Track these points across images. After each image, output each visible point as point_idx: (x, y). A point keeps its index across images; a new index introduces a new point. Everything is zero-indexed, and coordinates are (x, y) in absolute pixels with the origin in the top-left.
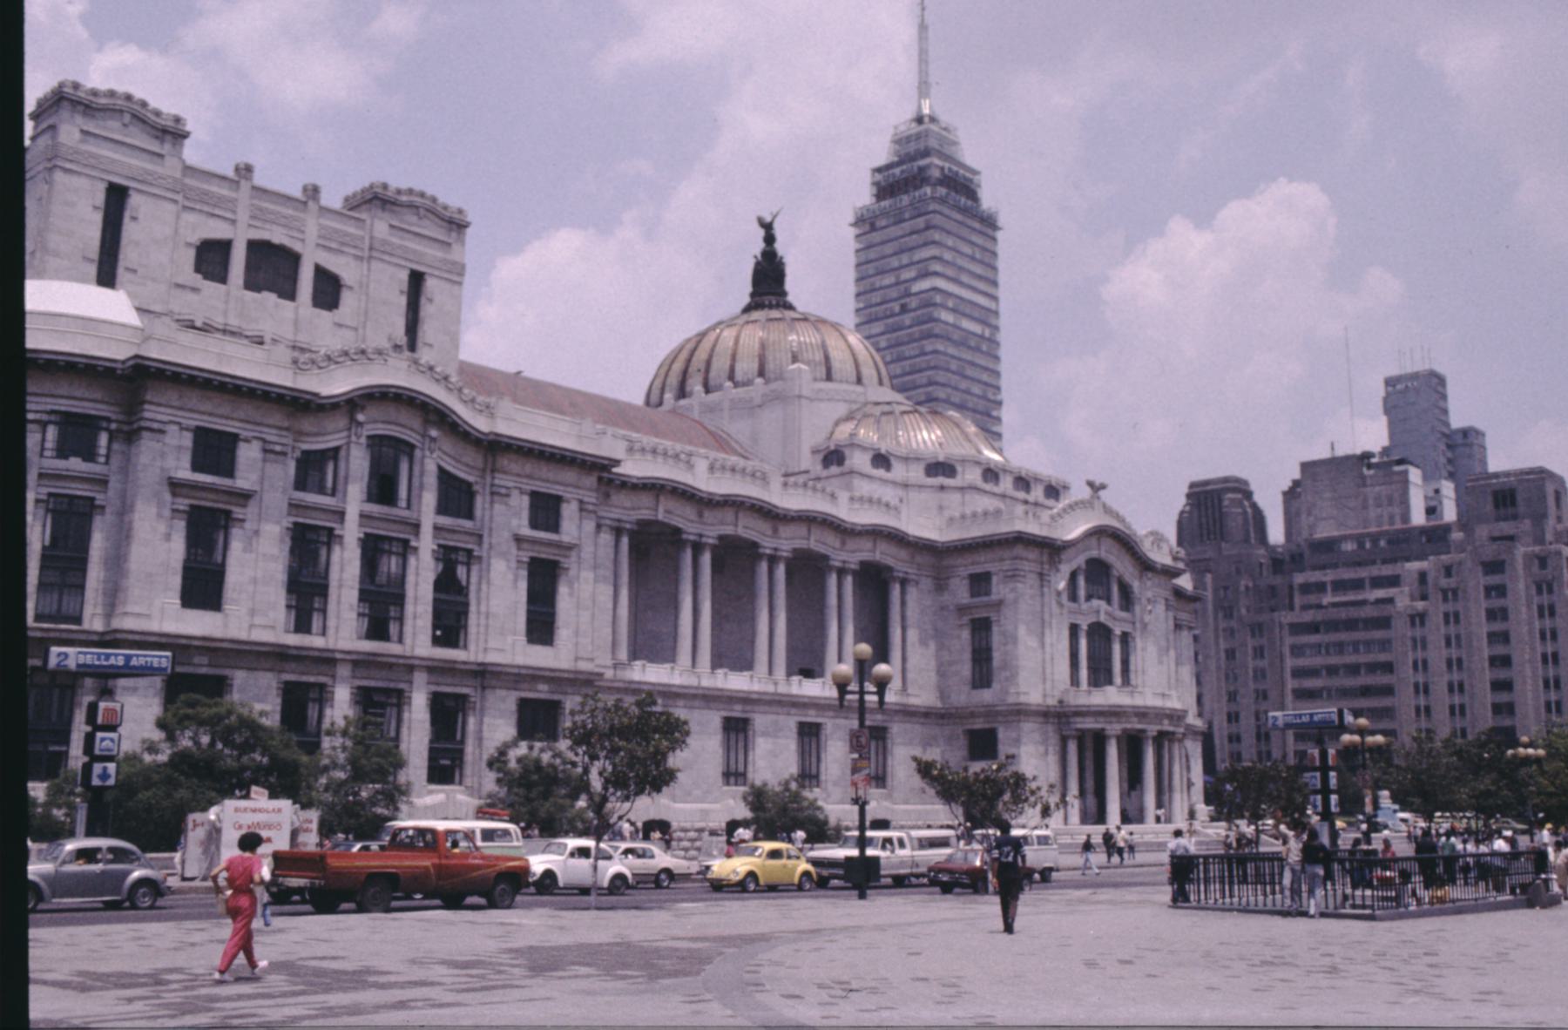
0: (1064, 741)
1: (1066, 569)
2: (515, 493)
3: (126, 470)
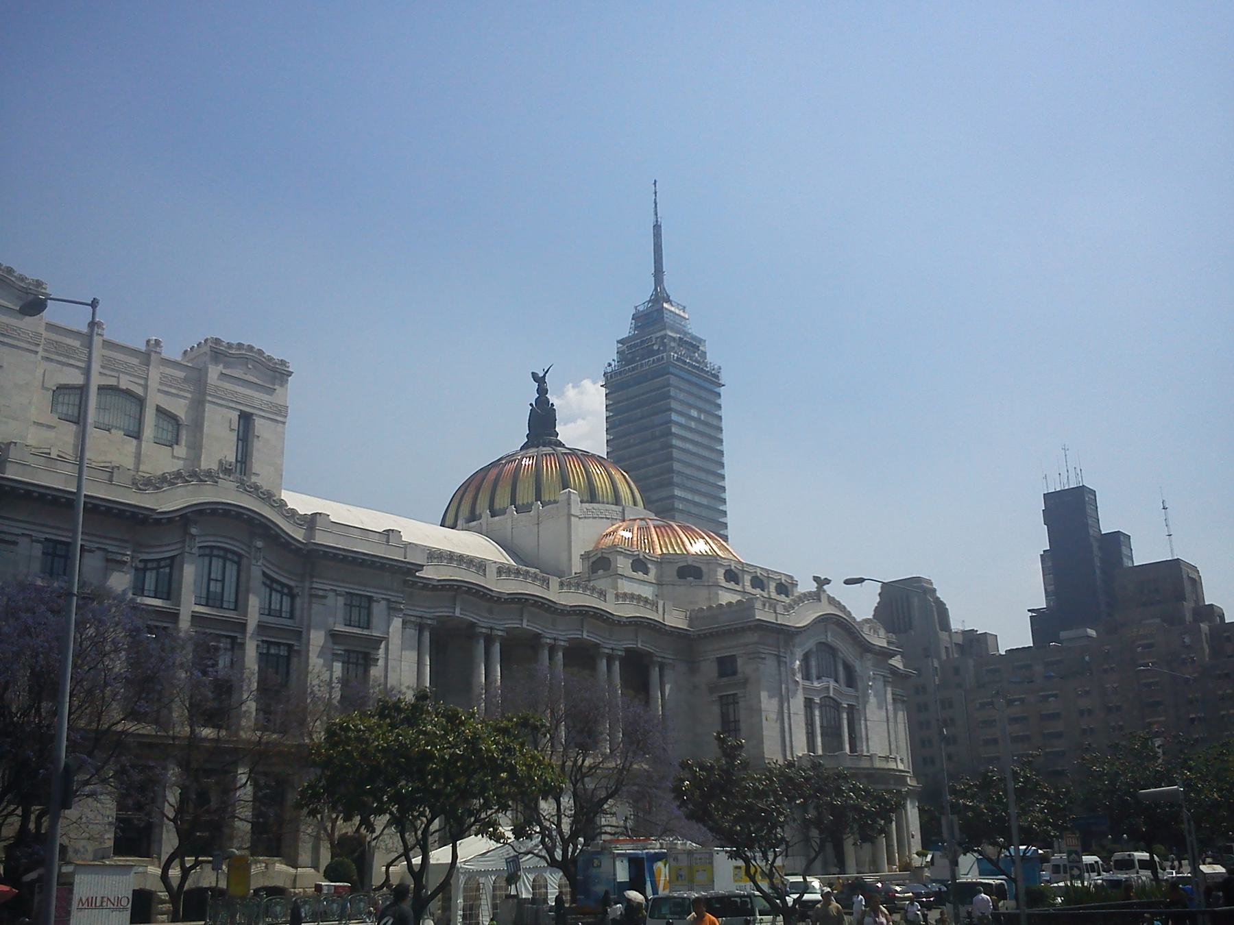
1: (799, 653)
2: (331, 595)
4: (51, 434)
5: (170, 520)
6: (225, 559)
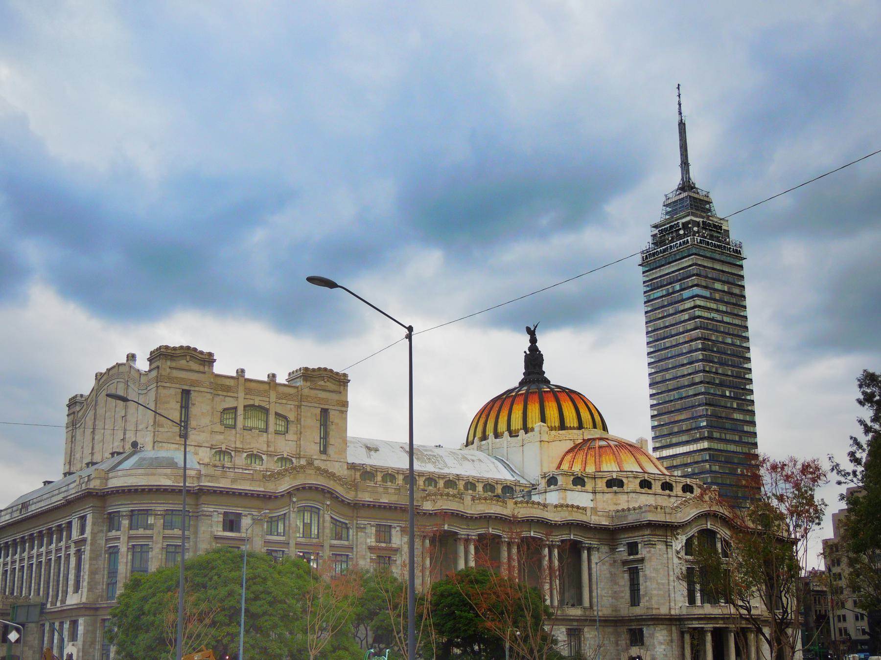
0: (682, 634)
3: (196, 533)
4: (221, 437)
5: (282, 496)
6: (311, 512)
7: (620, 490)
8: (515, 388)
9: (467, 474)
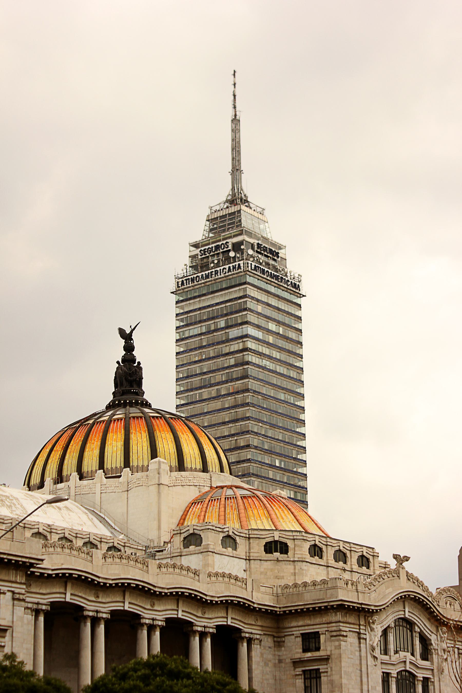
1: (379, 629)
7: (284, 556)
8: (95, 414)
9: (64, 525)
